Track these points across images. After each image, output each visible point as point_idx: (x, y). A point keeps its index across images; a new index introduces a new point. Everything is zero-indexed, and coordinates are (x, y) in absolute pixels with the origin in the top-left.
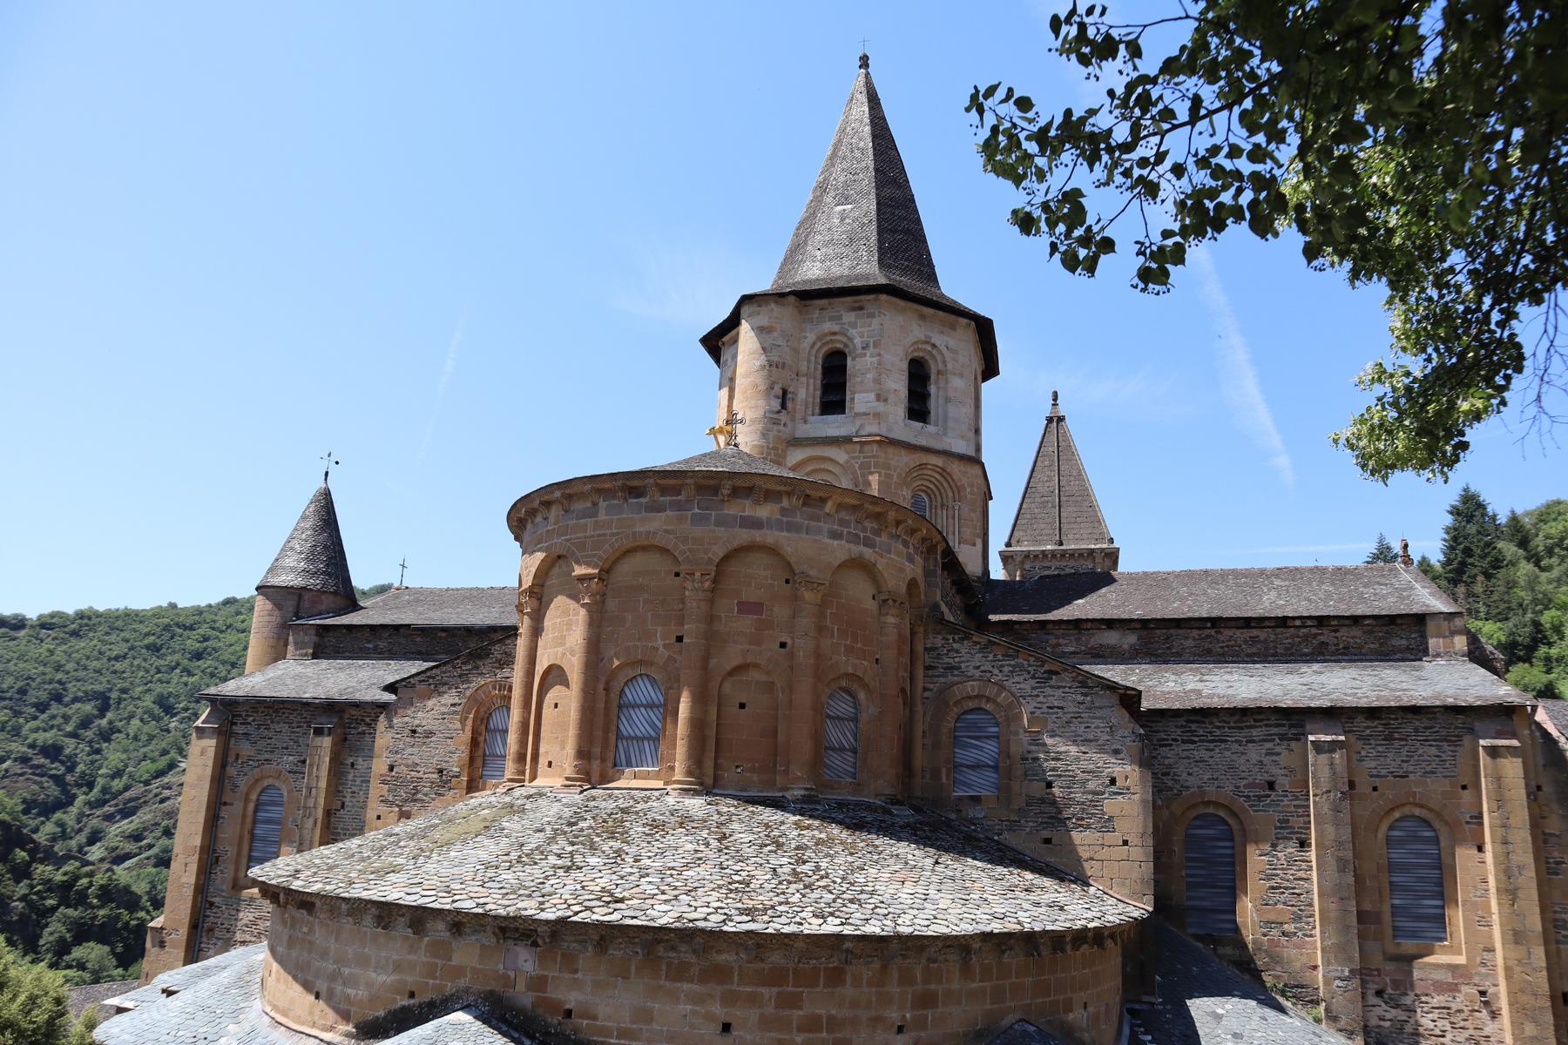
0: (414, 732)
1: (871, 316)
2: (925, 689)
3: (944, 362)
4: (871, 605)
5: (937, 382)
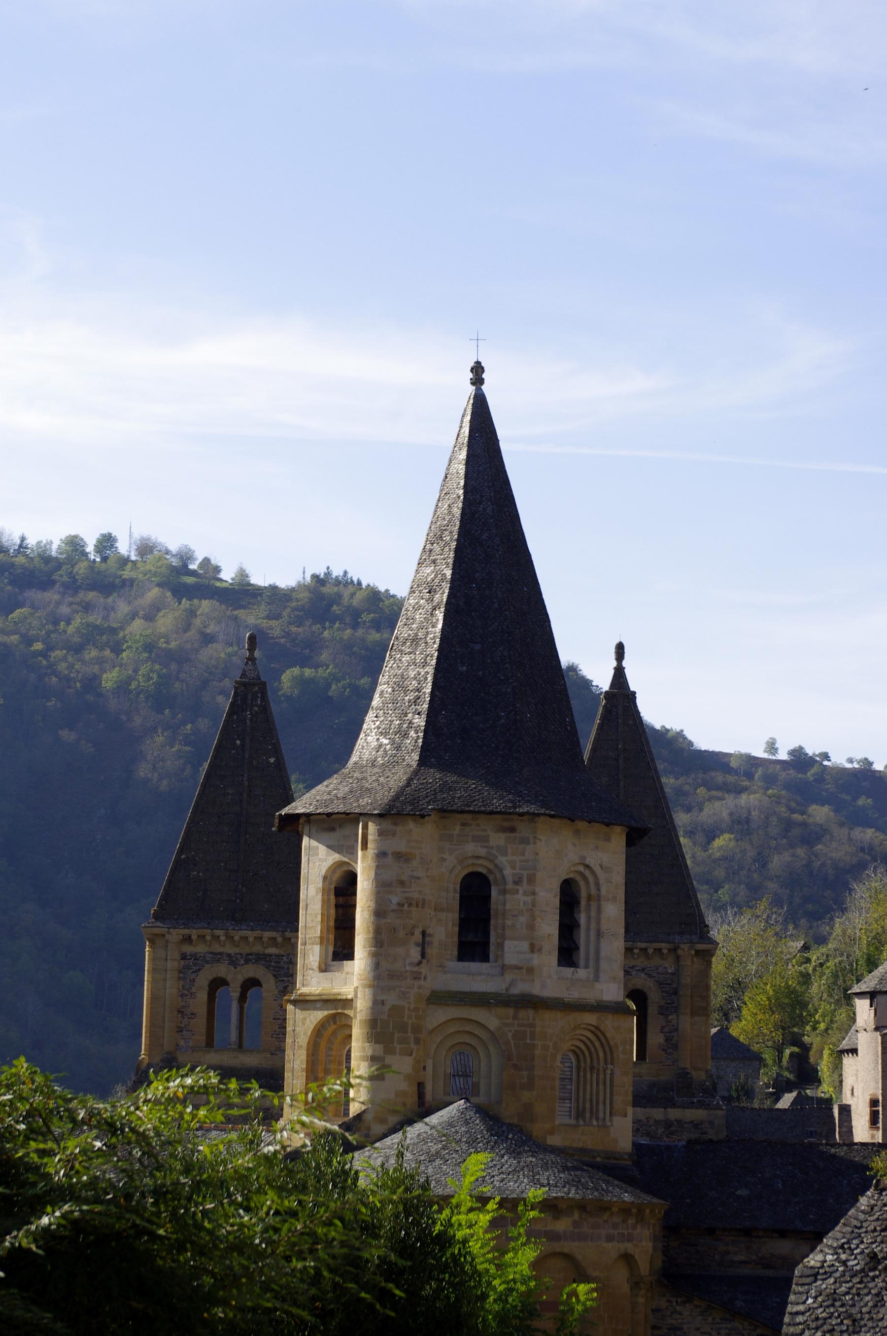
1: (525, 841)
3: (597, 885)
4: (626, 1288)
5: (588, 906)
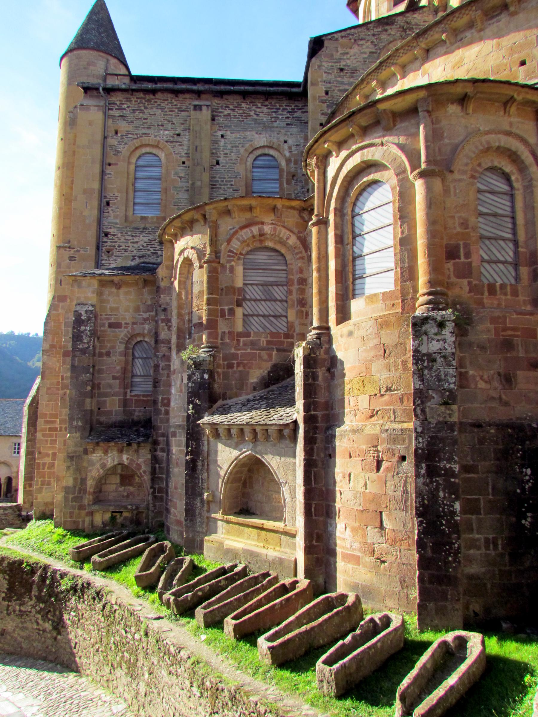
0: (342, 70)
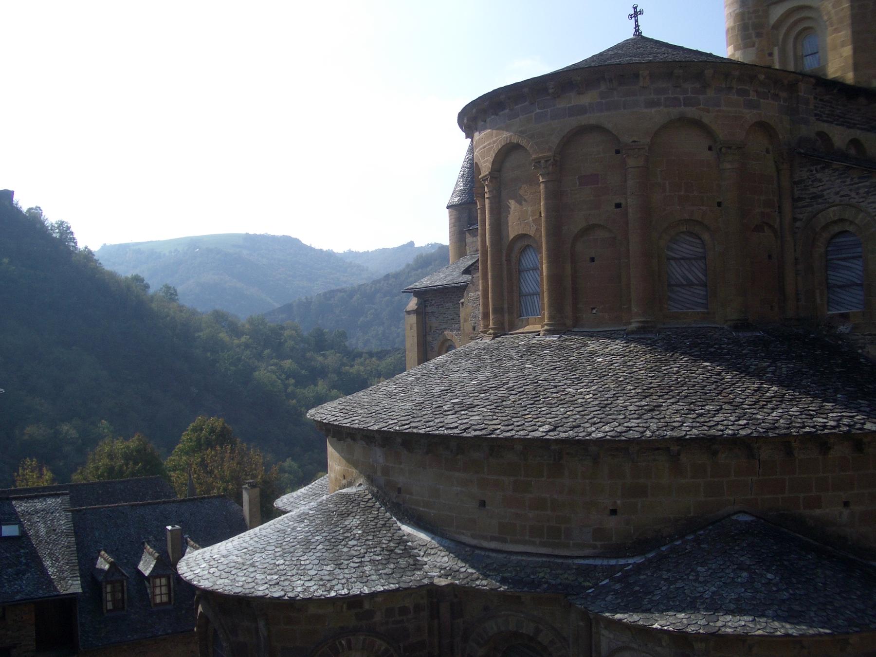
2: (795, 220)
